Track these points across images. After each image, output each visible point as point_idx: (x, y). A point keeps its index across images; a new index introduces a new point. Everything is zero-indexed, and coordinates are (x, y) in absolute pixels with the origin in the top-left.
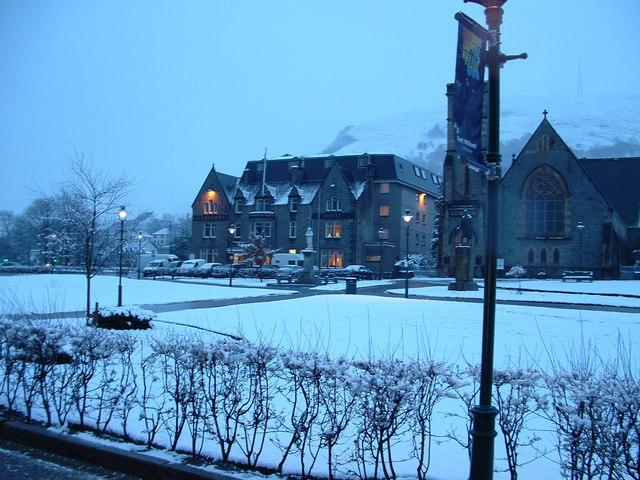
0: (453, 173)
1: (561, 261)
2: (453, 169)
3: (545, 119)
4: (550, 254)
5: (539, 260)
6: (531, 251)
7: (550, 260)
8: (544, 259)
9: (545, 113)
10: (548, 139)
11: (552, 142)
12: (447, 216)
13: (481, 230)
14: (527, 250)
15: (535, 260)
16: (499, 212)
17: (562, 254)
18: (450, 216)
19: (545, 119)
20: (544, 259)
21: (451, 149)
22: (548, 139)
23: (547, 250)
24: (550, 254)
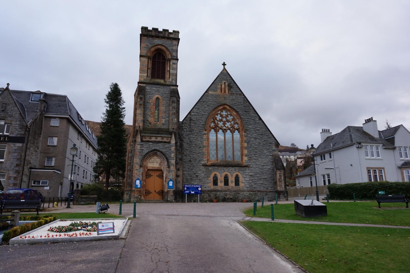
0: (144, 102)
1: (241, 185)
2: (145, 97)
3: (224, 69)
4: (231, 179)
5: (223, 184)
6: (215, 175)
7: (232, 184)
8: (226, 182)
9: (224, 64)
10: (227, 84)
11: (230, 87)
12: (139, 139)
13: (173, 155)
14: (212, 176)
15: (219, 183)
16: (186, 140)
17: (241, 179)
18: (142, 141)
19: (224, 69)
20: (226, 182)
21: (142, 80)
22: (227, 84)
23: (229, 174)
24: (231, 179)
